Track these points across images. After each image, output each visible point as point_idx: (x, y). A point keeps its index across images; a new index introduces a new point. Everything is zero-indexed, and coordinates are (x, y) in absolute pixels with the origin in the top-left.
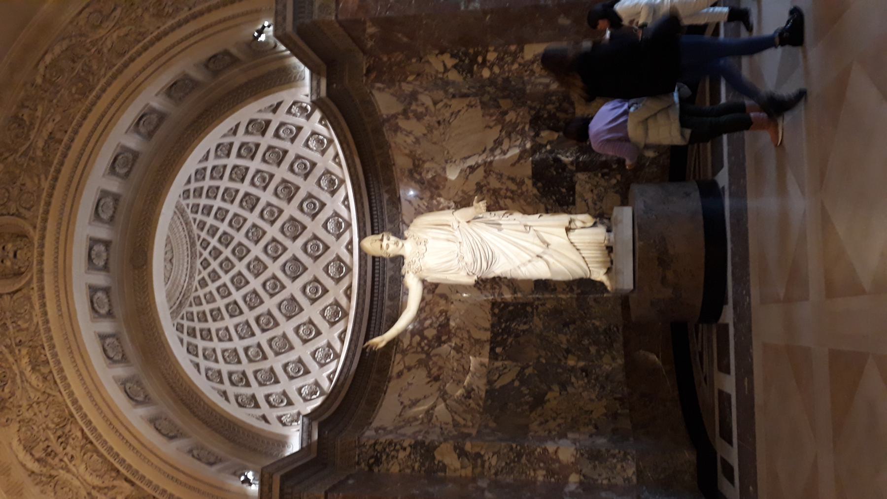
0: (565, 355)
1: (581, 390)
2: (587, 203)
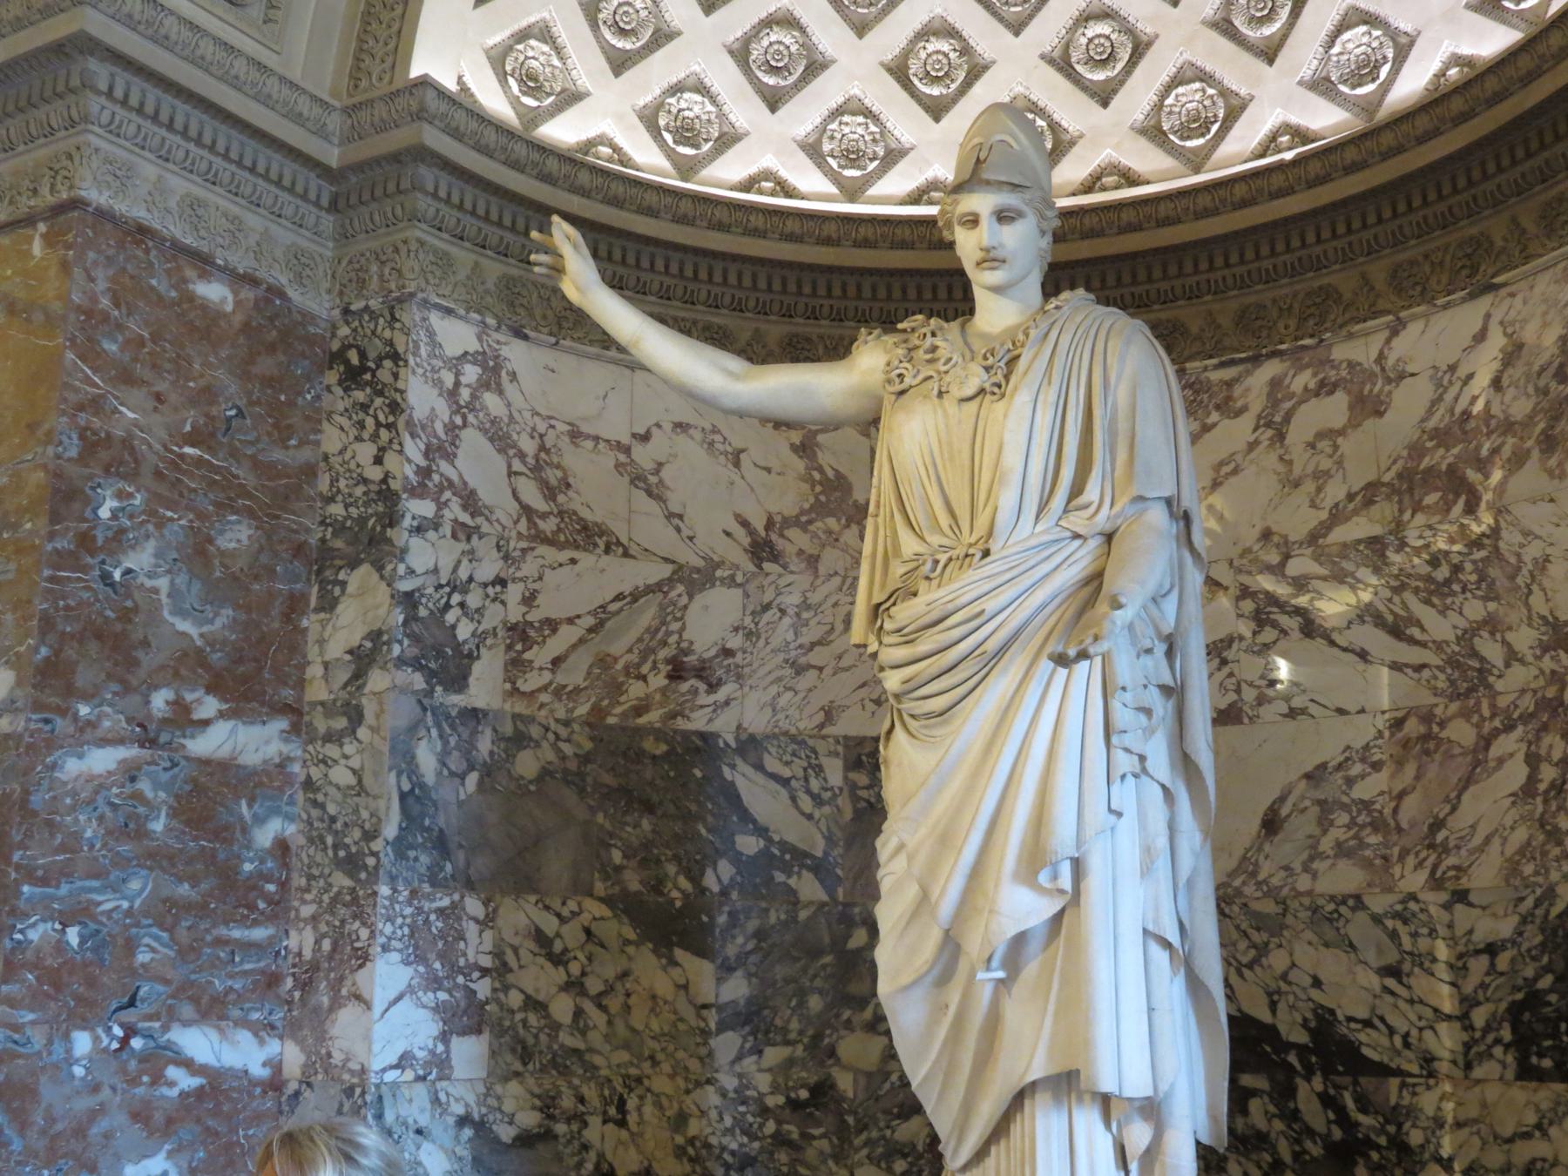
2: (1527, 1136)
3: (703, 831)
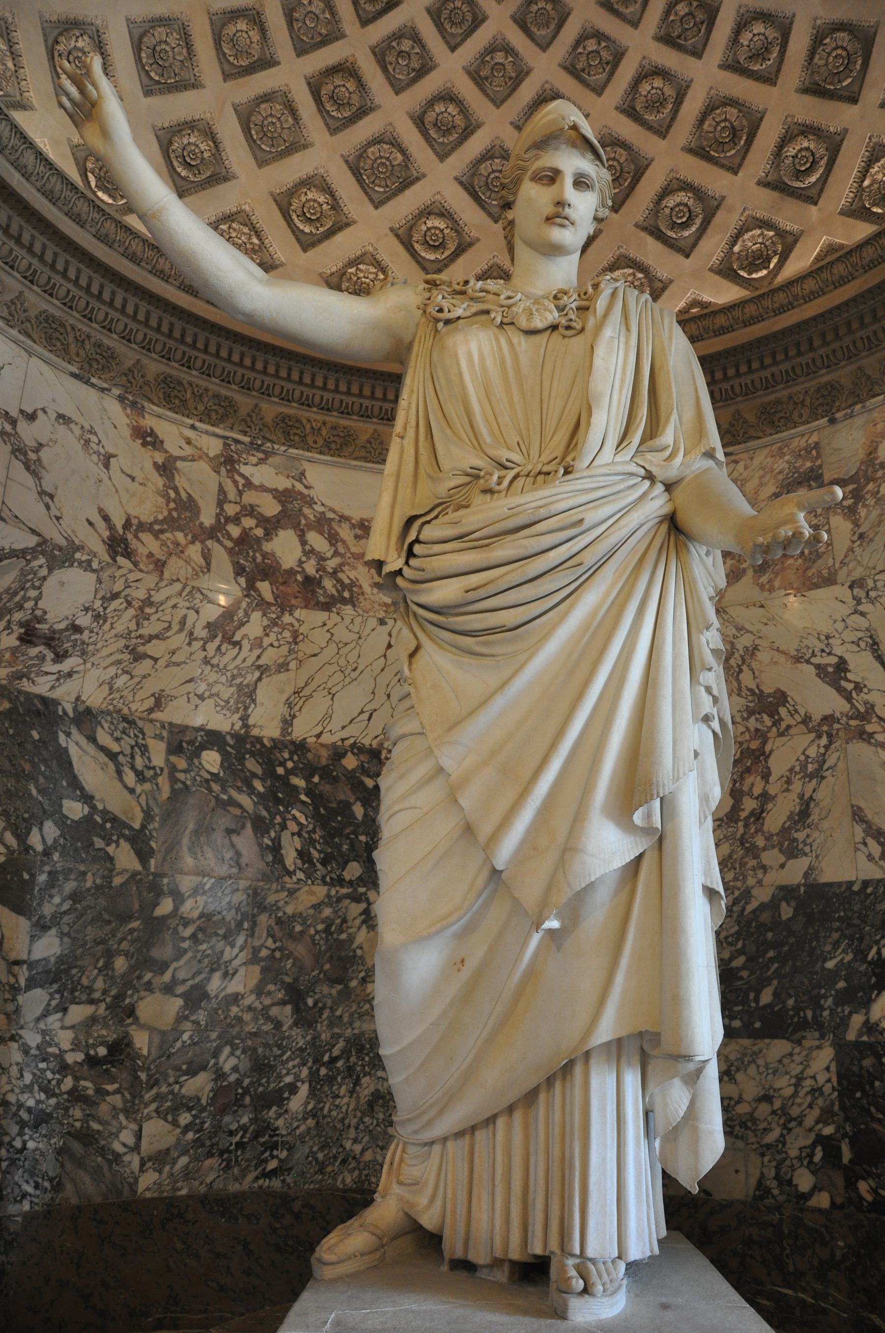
0: (180, 989)
1: (33, 1039)
3: (34, 792)
